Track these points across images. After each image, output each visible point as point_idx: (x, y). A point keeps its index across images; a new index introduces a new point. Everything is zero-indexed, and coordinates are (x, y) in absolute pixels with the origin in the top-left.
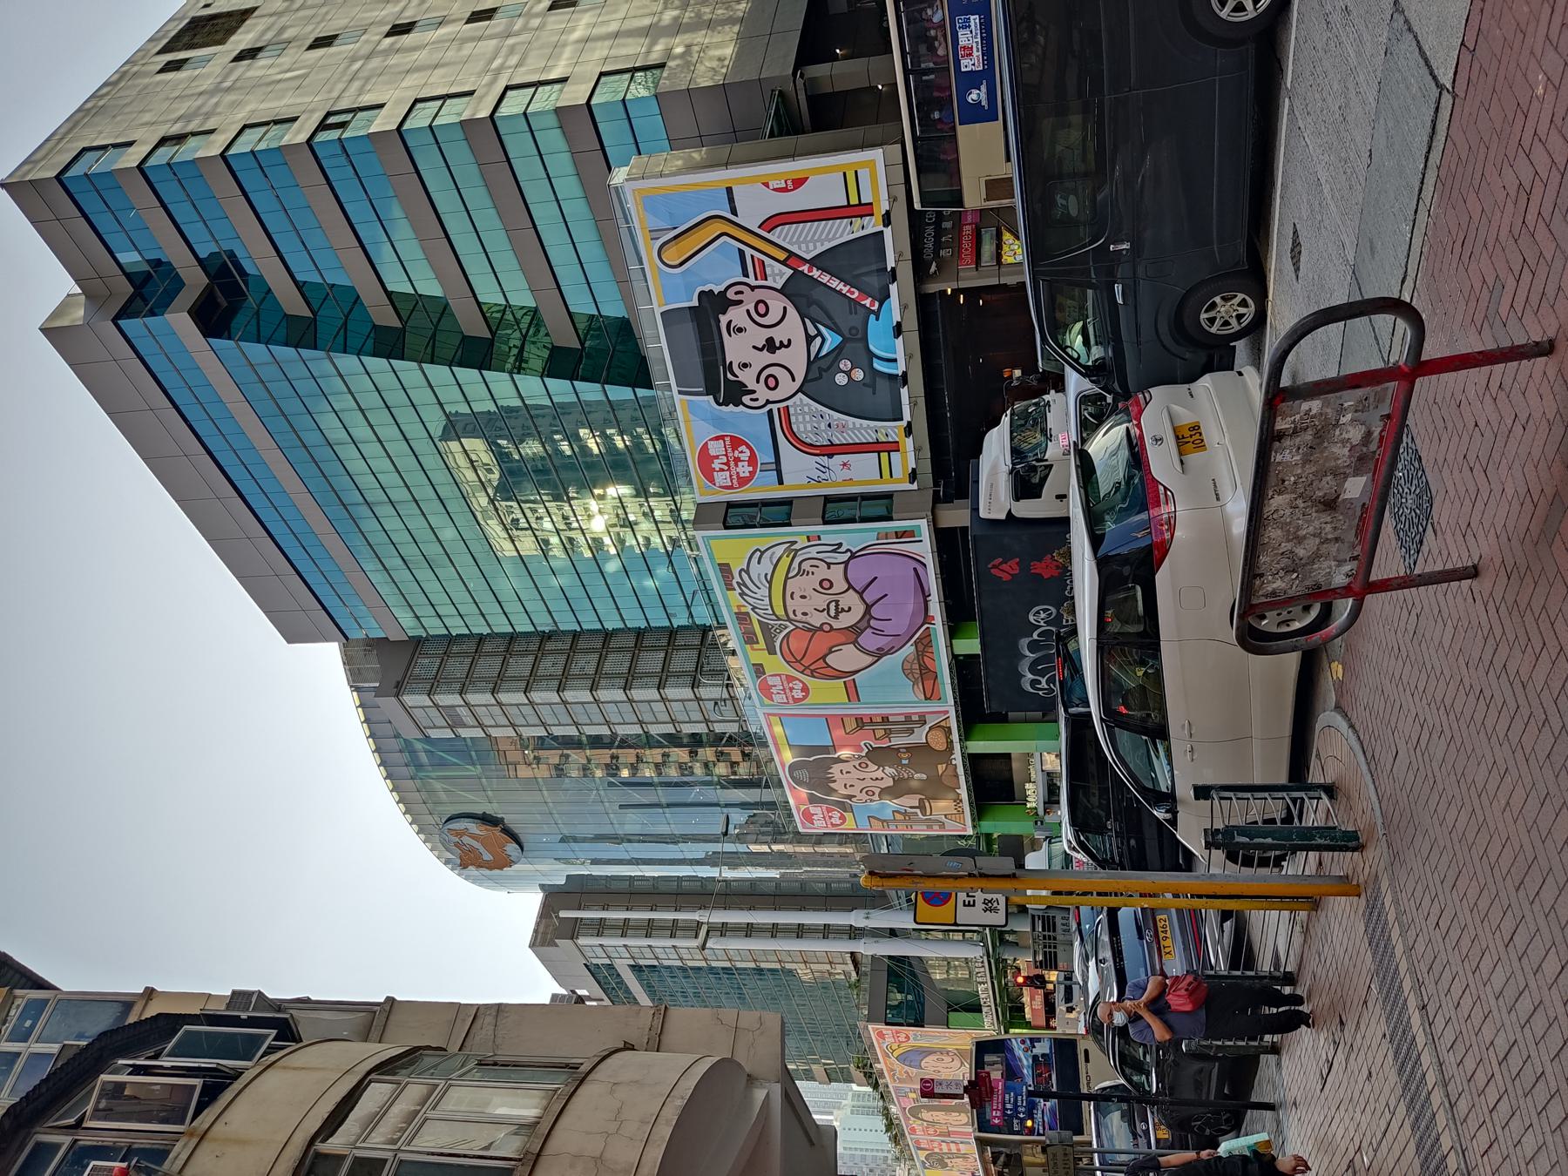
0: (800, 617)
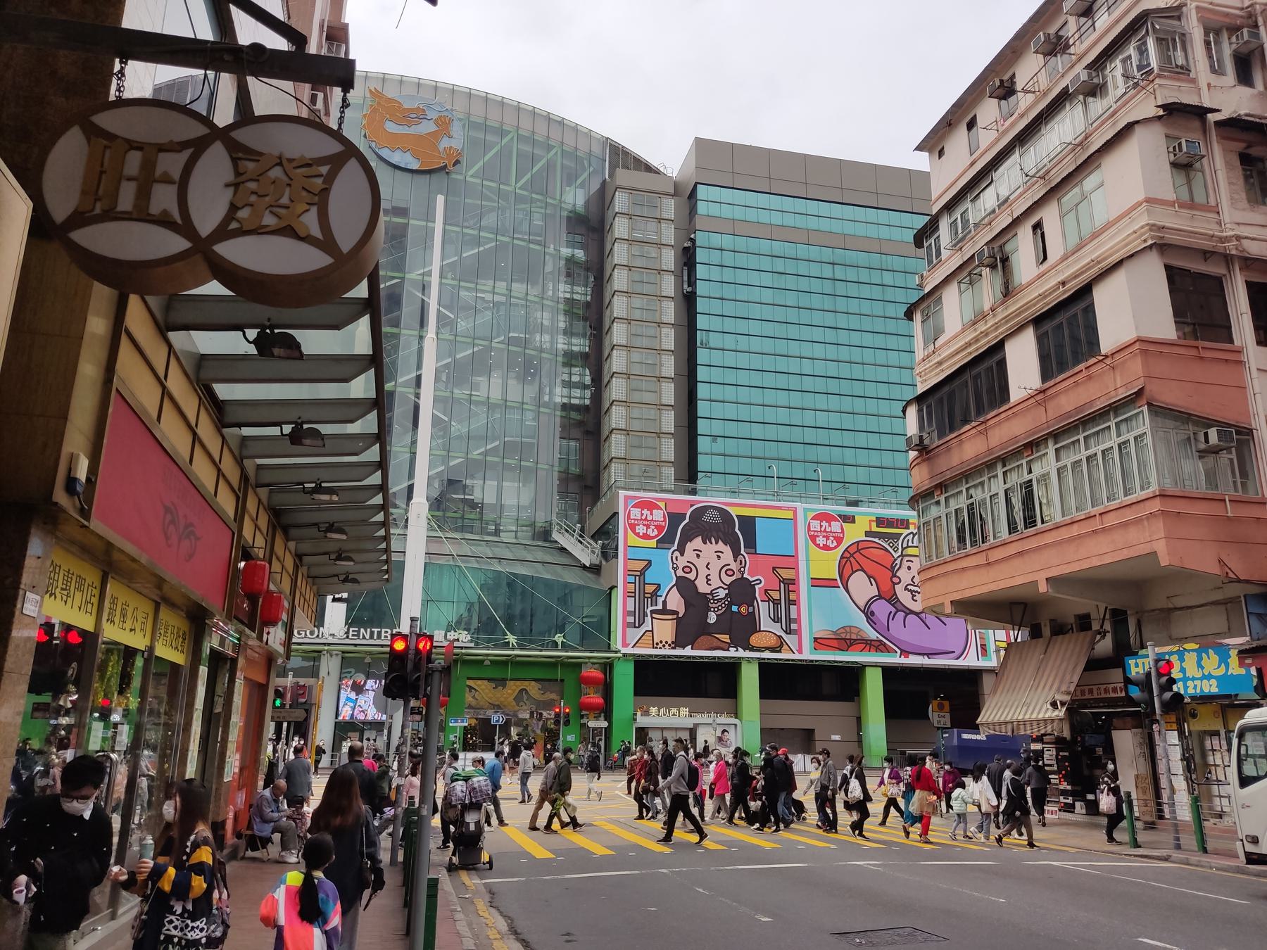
0: (905, 564)
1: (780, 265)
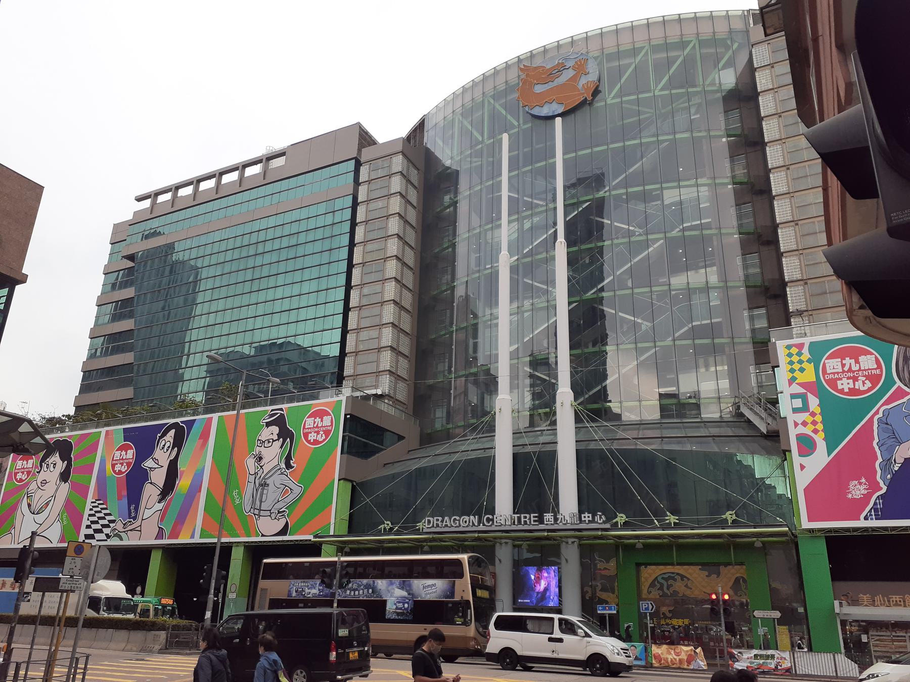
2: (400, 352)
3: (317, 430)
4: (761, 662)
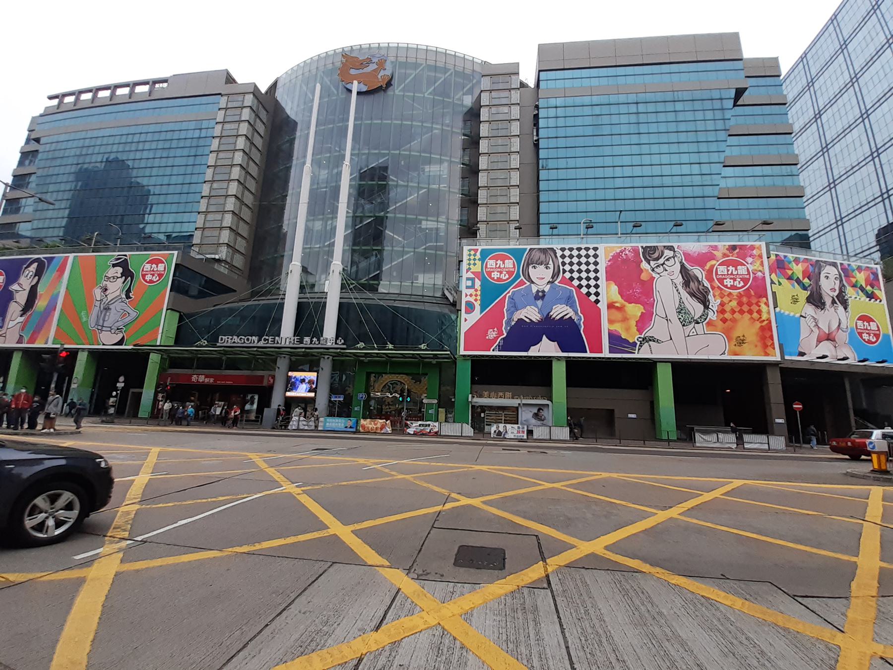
1: (597, 110)
2: (238, 233)
3: (152, 273)
4: (422, 428)
